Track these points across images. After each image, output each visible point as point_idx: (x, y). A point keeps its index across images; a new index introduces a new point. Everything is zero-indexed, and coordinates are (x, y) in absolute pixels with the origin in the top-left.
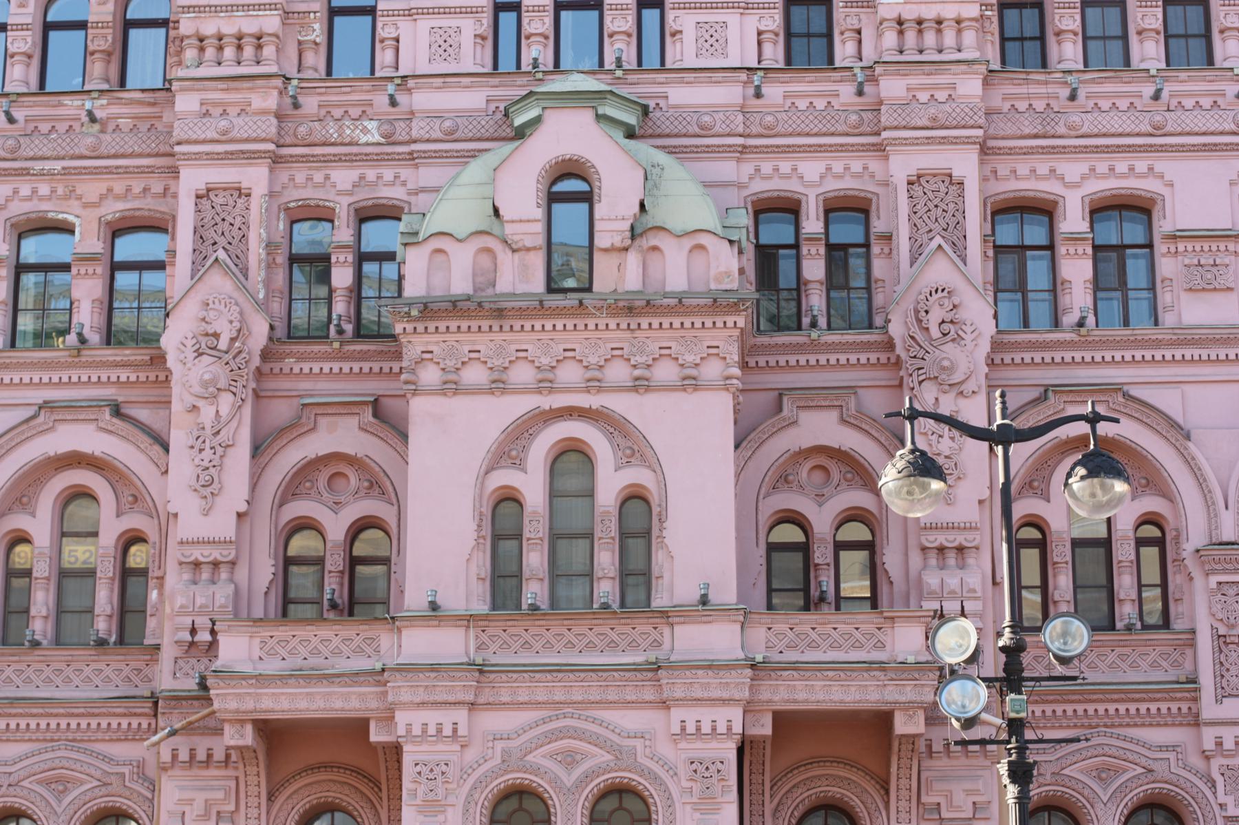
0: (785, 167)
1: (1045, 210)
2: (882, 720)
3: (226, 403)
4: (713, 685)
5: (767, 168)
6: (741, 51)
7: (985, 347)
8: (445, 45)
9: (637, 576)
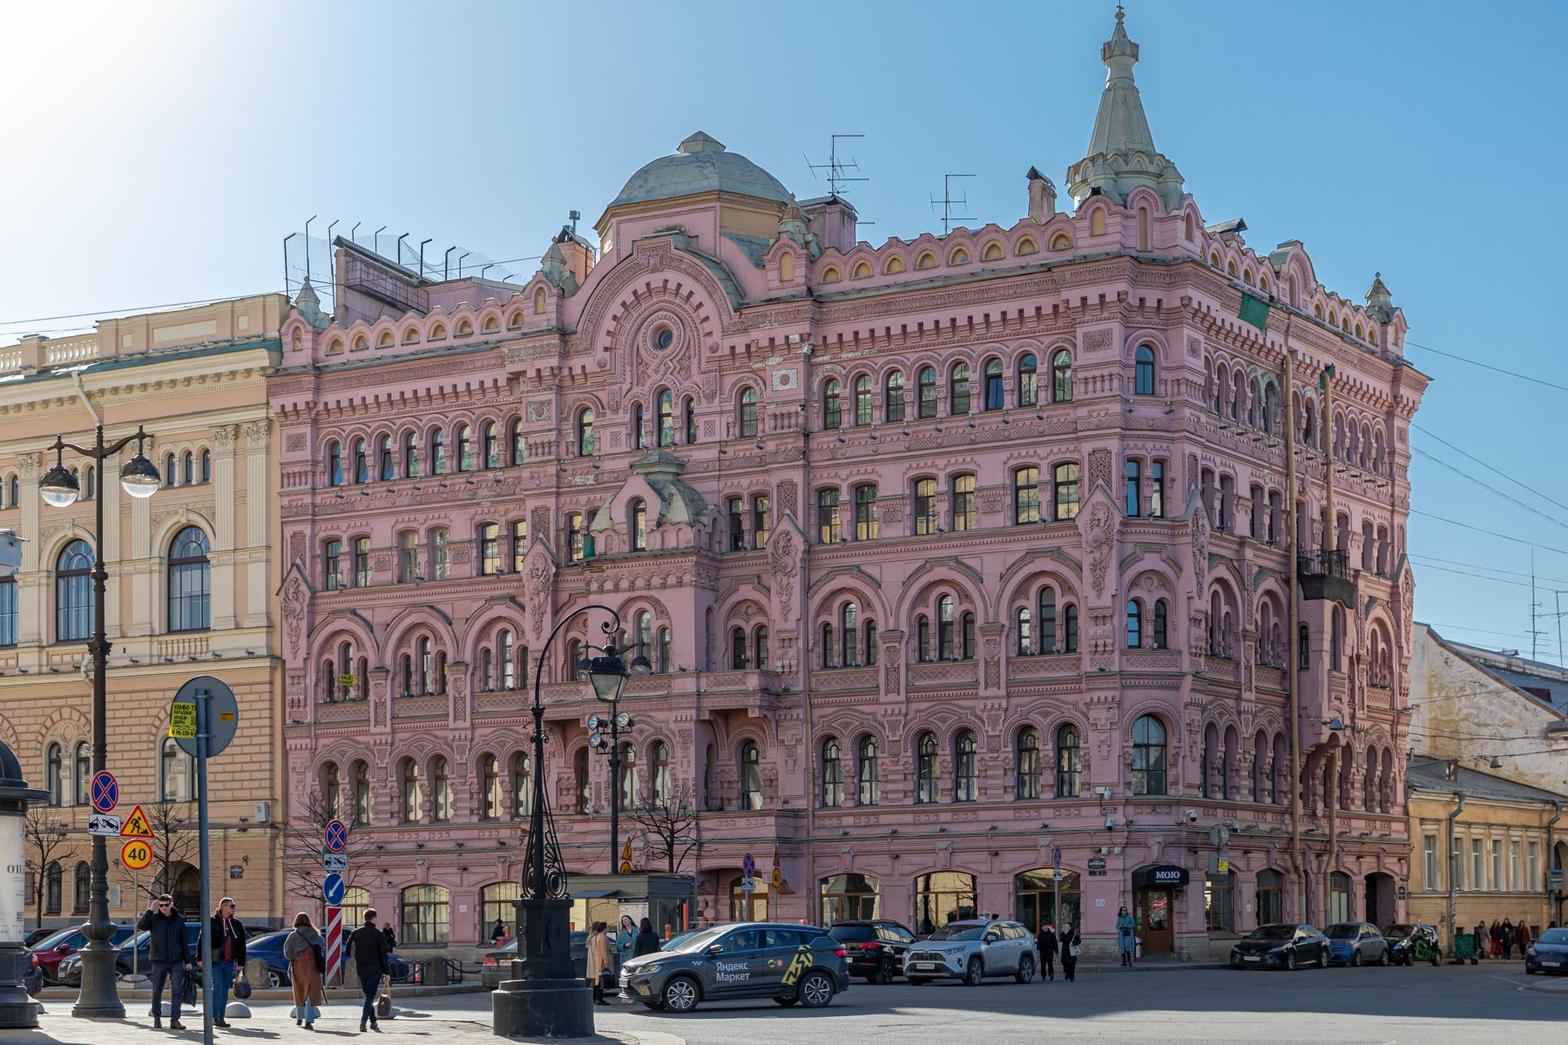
1: (834, 489)
2: (744, 711)
4: (684, 702)
6: (720, 434)
7: (800, 555)
8: (615, 440)
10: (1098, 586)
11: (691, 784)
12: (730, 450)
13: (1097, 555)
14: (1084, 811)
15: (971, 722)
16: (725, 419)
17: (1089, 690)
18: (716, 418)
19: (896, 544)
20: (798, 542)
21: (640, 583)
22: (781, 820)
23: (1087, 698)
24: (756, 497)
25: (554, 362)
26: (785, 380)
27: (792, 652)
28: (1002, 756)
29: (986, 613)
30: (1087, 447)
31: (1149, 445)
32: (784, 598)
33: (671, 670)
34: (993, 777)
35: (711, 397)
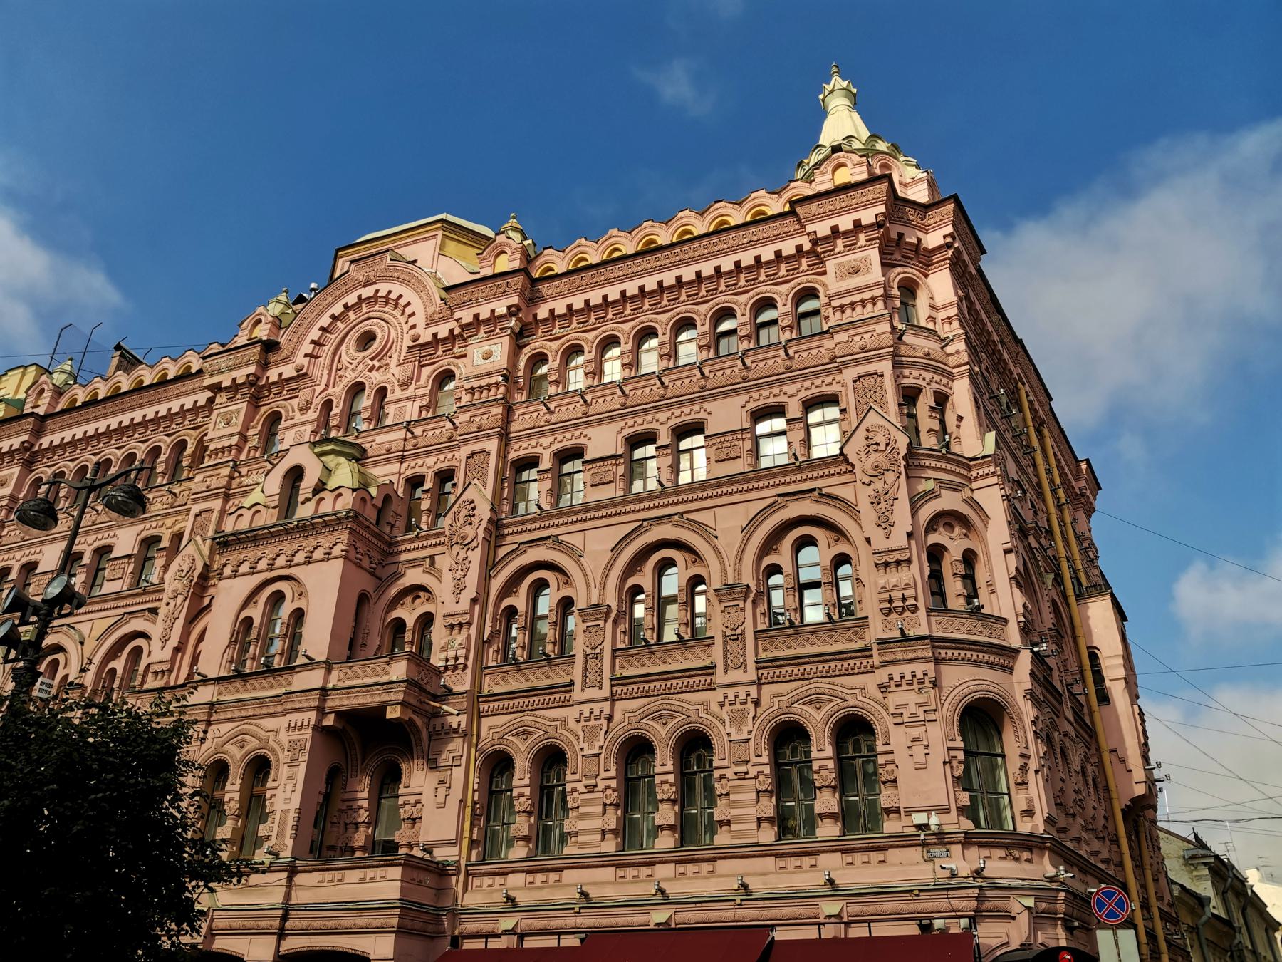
0: (420, 462)
2: (382, 709)
3: (180, 598)
5: (413, 464)
7: (484, 524)
9: (292, 652)
10: (885, 524)
11: (292, 815)
12: (418, 431)
13: (879, 485)
14: (893, 854)
15: (707, 722)
16: (418, 404)
17: (884, 664)
18: (409, 404)
19: (605, 507)
20: (484, 511)
21: (281, 561)
22: (415, 874)
23: (882, 675)
24: (445, 476)
25: (252, 369)
26: (488, 356)
27: (461, 638)
28: (753, 771)
29: (724, 573)
30: (849, 374)
31: (928, 375)
32: (459, 574)
33: (301, 660)
34: (740, 805)
35: (405, 385)
